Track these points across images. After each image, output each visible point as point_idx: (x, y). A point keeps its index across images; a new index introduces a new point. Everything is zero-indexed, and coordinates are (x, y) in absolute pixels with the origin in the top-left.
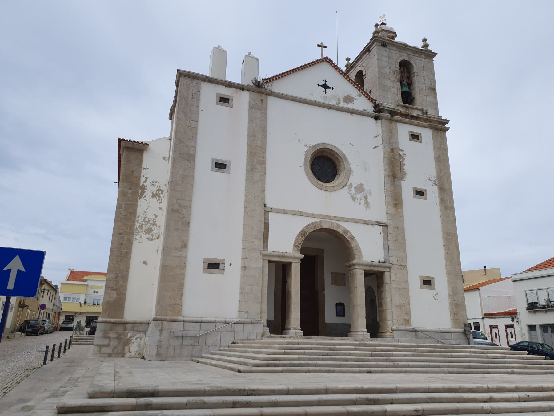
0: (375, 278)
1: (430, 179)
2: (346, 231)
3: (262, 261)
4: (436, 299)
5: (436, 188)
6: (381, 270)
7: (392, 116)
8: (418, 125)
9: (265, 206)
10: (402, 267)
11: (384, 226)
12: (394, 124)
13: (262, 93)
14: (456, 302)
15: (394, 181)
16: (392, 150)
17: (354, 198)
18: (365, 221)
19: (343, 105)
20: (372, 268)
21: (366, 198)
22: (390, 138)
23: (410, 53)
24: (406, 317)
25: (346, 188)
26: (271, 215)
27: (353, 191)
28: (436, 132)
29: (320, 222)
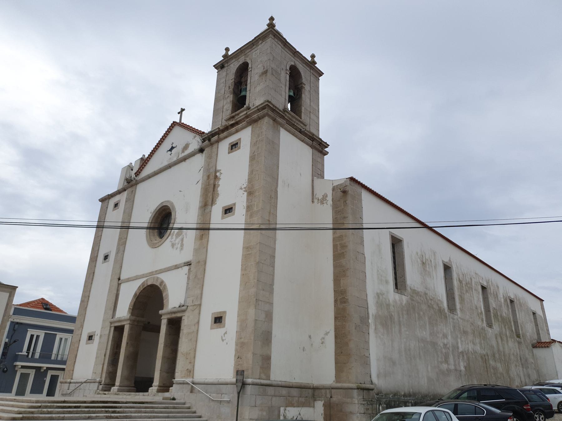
0: (175, 324)
1: (241, 189)
2: (162, 282)
3: (109, 328)
4: (223, 340)
5: (246, 193)
6: (179, 315)
7: (209, 140)
8: (237, 131)
9: (119, 279)
10: (195, 307)
11: (189, 264)
12: (215, 146)
13: (132, 186)
14: (242, 340)
15: (205, 210)
16: (208, 177)
17: (173, 245)
18: (176, 266)
19: (182, 155)
20: (173, 316)
21: (182, 240)
22: (209, 165)
23: (248, 51)
24: (189, 367)
25: (170, 237)
26: (123, 286)
27: (174, 237)
28: (256, 124)
29: (147, 280)
